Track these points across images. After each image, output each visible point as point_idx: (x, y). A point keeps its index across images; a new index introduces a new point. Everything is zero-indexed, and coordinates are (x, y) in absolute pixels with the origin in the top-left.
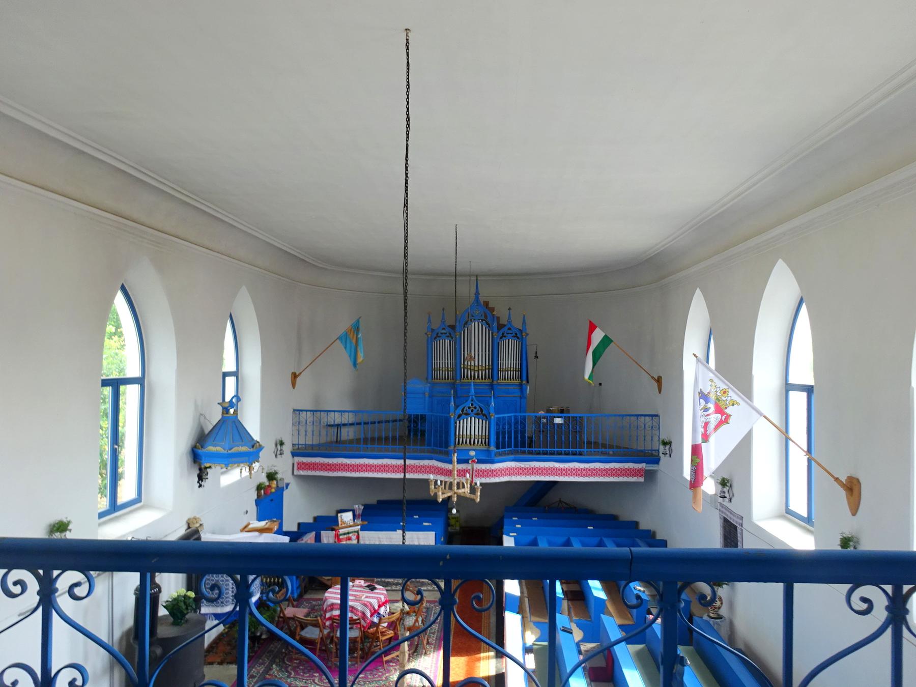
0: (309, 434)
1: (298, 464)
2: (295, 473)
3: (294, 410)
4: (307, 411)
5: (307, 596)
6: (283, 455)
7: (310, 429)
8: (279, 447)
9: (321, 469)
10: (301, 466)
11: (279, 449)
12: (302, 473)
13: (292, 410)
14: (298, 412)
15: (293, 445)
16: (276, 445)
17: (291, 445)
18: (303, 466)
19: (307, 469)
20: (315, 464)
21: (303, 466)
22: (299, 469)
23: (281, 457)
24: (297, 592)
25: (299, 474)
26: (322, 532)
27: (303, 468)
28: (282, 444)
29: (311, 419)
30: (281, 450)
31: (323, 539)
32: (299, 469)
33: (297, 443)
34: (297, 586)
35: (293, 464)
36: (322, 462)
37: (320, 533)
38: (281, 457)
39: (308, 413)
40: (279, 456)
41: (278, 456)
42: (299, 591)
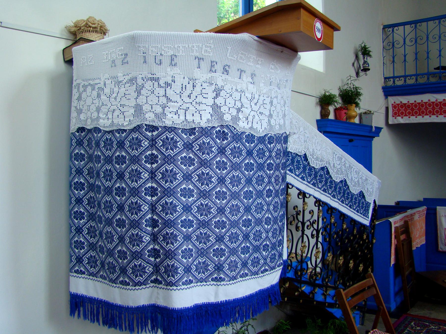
0: (410, 58)
1: (394, 106)
2: (390, 122)
3: (385, 27)
4: (404, 24)
5: (415, 312)
6: (368, 72)
7: (410, 50)
8: (361, 56)
9: (432, 113)
10: (399, 110)
11: (361, 62)
12: (401, 120)
13: (382, 27)
14: (391, 29)
15: (385, 78)
16: (357, 57)
17: (383, 80)
18: (402, 110)
19: (409, 113)
20: (422, 106)
21: (402, 110)
22: (395, 115)
23: (366, 75)
24: (395, 301)
25: (396, 122)
26: (438, 207)
27: (402, 113)
28: (365, 52)
29: (413, 35)
30: (365, 62)
31: (440, 220)
32: (395, 115)
33: (392, 75)
34: (397, 289)
35: (387, 109)
36: (433, 100)
37: (435, 210)
38: (366, 75)
39: (407, 27)
40: (361, 73)
41: (361, 73)
42: (399, 300)
